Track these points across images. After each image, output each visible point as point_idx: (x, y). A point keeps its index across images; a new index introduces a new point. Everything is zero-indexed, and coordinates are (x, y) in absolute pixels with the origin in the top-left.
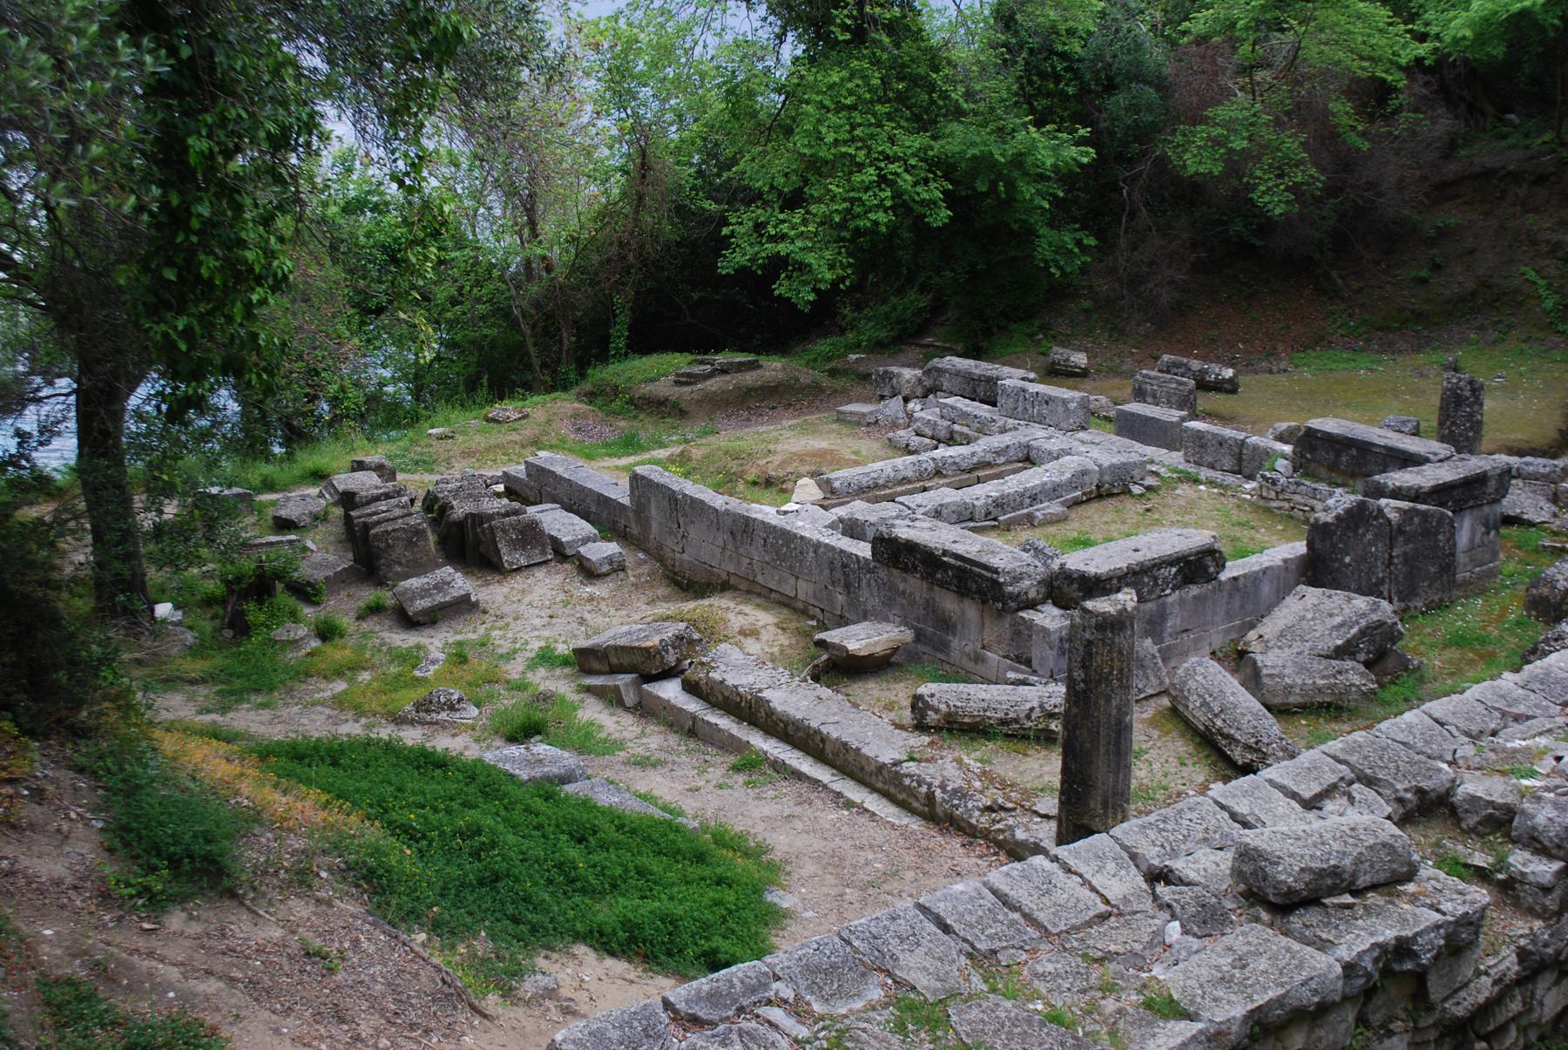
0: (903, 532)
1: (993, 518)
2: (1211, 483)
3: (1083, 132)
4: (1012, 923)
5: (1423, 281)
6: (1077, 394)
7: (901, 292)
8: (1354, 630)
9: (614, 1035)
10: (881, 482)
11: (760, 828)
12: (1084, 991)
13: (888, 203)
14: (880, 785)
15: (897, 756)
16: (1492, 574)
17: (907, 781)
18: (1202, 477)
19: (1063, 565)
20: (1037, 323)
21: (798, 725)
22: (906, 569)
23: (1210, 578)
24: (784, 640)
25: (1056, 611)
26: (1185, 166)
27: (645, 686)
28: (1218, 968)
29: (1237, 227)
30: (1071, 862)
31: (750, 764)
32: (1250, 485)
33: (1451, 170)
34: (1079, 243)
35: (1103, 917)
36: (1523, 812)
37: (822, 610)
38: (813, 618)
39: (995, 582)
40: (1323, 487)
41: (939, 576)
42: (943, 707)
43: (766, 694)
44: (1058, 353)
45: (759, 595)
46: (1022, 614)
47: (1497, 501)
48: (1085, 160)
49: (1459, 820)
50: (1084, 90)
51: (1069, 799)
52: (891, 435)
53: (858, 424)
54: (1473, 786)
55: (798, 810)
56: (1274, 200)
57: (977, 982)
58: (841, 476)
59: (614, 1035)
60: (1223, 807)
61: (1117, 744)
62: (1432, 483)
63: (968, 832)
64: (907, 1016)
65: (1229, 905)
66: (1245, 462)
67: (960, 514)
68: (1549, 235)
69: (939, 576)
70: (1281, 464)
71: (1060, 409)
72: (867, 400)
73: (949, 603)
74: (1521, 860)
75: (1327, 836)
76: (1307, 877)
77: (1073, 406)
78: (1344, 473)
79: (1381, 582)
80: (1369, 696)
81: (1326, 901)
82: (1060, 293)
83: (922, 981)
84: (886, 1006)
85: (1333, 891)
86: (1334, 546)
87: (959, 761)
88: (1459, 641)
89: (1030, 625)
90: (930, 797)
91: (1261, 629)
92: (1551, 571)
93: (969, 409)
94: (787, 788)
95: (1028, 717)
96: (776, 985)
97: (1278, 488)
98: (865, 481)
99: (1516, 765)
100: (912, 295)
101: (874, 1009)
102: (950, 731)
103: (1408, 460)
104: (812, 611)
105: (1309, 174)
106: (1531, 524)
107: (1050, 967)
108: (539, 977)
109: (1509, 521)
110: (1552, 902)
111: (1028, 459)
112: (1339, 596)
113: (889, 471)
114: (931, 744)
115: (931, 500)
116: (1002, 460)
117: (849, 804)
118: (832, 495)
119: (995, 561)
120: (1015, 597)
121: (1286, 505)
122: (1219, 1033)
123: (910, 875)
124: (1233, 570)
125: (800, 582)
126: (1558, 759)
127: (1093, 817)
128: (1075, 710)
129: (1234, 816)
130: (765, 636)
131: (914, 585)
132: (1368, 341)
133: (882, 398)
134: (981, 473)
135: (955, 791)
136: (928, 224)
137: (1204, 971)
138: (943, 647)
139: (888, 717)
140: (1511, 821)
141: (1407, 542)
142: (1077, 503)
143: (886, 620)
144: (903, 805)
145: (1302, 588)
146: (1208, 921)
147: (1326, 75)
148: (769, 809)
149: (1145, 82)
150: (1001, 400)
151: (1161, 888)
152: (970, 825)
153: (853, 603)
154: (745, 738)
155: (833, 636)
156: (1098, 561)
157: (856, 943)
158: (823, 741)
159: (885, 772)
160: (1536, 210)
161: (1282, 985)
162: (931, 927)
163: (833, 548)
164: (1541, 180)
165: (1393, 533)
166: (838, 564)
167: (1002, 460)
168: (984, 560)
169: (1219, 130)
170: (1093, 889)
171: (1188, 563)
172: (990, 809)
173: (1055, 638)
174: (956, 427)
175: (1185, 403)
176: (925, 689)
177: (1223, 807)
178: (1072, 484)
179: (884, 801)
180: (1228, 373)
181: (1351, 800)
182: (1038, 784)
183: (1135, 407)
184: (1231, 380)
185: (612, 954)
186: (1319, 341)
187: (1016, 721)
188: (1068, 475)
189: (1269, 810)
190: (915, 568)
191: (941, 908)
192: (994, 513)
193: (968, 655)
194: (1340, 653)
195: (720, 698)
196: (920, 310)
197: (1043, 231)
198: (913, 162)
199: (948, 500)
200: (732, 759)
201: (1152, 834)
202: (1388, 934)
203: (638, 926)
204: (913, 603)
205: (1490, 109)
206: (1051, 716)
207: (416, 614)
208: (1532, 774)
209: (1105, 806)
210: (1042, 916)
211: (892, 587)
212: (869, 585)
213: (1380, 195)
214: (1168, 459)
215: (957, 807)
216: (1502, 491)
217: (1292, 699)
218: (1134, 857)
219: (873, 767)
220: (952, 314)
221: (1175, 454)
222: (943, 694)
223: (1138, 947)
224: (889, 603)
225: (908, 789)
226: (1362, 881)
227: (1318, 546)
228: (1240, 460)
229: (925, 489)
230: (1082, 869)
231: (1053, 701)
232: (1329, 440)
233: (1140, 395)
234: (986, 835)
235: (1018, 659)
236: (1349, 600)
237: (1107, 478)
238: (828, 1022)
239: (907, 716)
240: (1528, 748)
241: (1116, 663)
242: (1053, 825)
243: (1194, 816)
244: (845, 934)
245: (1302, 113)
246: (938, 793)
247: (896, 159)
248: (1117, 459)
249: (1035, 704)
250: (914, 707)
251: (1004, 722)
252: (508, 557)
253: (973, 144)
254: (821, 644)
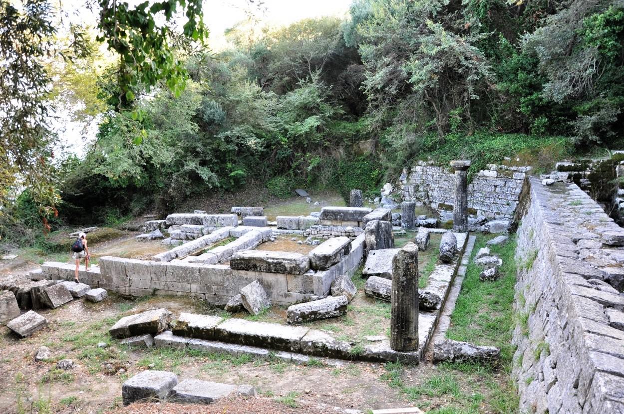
19: (314, 255)
27: (155, 337)
37: (205, 294)
43: (220, 327)
73: (270, 278)
97: (318, 230)
121: (321, 235)
174: (188, 234)
207: (23, 333)
212: (228, 280)
252: (56, 302)
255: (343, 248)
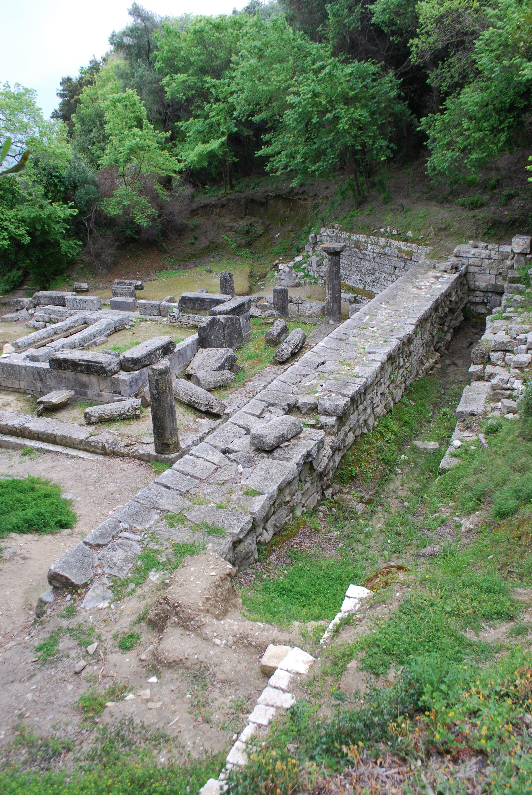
0: (61, 355)
1: (82, 345)
2: (152, 320)
3: (71, 204)
4: (189, 480)
5: (193, 244)
6: (96, 297)
7: (10, 271)
8: (223, 360)
9: (73, 560)
10: (36, 340)
11: (44, 474)
12: (224, 495)
13: (7, 237)
14: (82, 447)
15: (86, 436)
16: (250, 335)
17: (93, 444)
18: (148, 319)
19: (124, 357)
20: (65, 275)
21: (43, 434)
22: (65, 369)
23: (172, 352)
24: (21, 404)
25: (125, 373)
26: (109, 213)
28: (261, 475)
29: (129, 232)
30: (198, 454)
31: (28, 452)
32: (165, 319)
33: (194, 206)
34: (76, 244)
35: (216, 470)
36: (321, 404)
38: (29, 394)
39: (102, 367)
40: (190, 315)
41: (79, 369)
42: (97, 415)
43: (26, 425)
44: (77, 285)
45: (4, 390)
46: (114, 376)
47: (248, 311)
48: (75, 214)
49: (301, 411)
50: (67, 188)
51: (158, 435)
52: (26, 323)
53: (11, 321)
54: (303, 400)
55: (55, 464)
56: (142, 221)
57: (188, 503)
58: (20, 340)
59: (73, 560)
60: (235, 424)
61: (172, 412)
62: (230, 308)
63: (122, 456)
64: (172, 521)
65: (253, 455)
66: (161, 312)
67: (70, 346)
68: (229, 224)
69: (79, 369)
70: (176, 310)
71: (91, 303)
72: (11, 312)
73: (84, 378)
74: (323, 419)
75: (276, 425)
76: (276, 439)
77: (95, 302)
78: (197, 310)
79: (223, 343)
80: (233, 380)
81: (281, 446)
82: (72, 263)
83: (171, 508)
84: (162, 520)
85: (282, 442)
86: (208, 334)
87: (109, 432)
88: (250, 357)
89: (118, 380)
90: (104, 447)
91: (191, 365)
92: (271, 330)
93: (55, 309)
94: (47, 457)
95: (128, 411)
96: (121, 524)
98: (30, 341)
99: (310, 390)
100: (15, 272)
101: (158, 522)
102: (101, 422)
103: (218, 302)
104: (28, 392)
105: (152, 211)
106: (256, 317)
107: (209, 491)
108: (9, 549)
109: (251, 316)
110: (335, 430)
111: (86, 323)
112: (214, 350)
113: (38, 336)
114: (96, 428)
115: (59, 343)
116: (76, 325)
117: (73, 457)
118: (18, 348)
119: (99, 360)
120: (110, 371)
121: (180, 324)
122: (272, 496)
123: (108, 475)
124: (179, 347)
125: (21, 382)
126: (322, 386)
127: (168, 439)
128: (155, 405)
129: (239, 426)
130: (13, 405)
131: (69, 374)
132: (179, 266)
133: (17, 310)
134: (71, 331)
135: (112, 443)
136: (23, 244)
137: (258, 478)
138: (85, 394)
139: (76, 423)
140: (317, 407)
141: (228, 328)
142: (109, 335)
143: (59, 389)
144: (93, 452)
145: (200, 350)
146: (249, 462)
147: (152, 176)
148: (44, 466)
149: (89, 184)
150: (67, 304)
151: (227, 454)
152: (121, 453)
153: (45, 385)
154: (23, 443)
155: (44, 398)
156: (135, 353)
157: (141, 502)
158: (55, 437)
159: (83, 442)
160: (223, 216)
161: (283, 475)
162: (164, 489)
163: (32, 367)
164: (223, 206)
165: (224, 326)
166: (36, 372)
167: (76, 325)
168: (95, 360)
169: (119, 199)
170: (209, 461)
171: (164, 348)
172: (127, 446)
173: (128, 382)
174: (52, 316)
175: (132, 295)
176: (88, 410)
177: (235, 424)
178: (106, 329)
179: (85, 452)
180: (139, 283)
181: (270, 412)
182: (140, 433)
183: (115, 299)
184: (141, 285)
185: (24, 533)
186: (163, 268)
187: (124, 414)
188: (104, 326)
189: (249, 422)
190: (68, 368)
191: (164, 481)
192: (82, 344)
193: (95, 395)
194: (221, 368)
195: (7, 431)
196: (19, 277)
197: (62, 241)
198: (13, 220)
199: (65, 342)
200: (20, 452)
201: (218, 438)
202: (304, 452)
203: (31, 520)
204: (69, 380)
205: (200, 184)
206: (136, 409)
208: (317, 392)
209: (171, 435)
210: (197, 475)
211: (60, 377)
213: (174, 216)
214: (135, 315)
215: (115, 448)
216: (249, 308)
217: (211, 386)
218: (215, 447)
219: (78, 442)
220: (32, 276)
221: (136, 313)
222: (95, 410)
223: (233, 476)
224: (60, 383)
225: (95, 447)
226: (289, 437)
227: (202, 334)
228: (160, 311)
229: (52, 341)
230: (202, 456)
231: (135, 404)
232: (190, 299)
233: (115, 294)
234: (128, 455)
235: (115, 393)
236: (218, 350)
237: (117, 325)
238: (145, 532)
239: (83, 421)
240: (312, 384)
241: (167, 386)
242: (153, 445)
243: (227, 429)
244: (136, 500)
245: (144, 191)
246: (106, 445)
247: (6, 220)
248: (119, 318)
249: (130, 406)
250: (85, 417)
251: (120, 415)
253: (33, 212)
254: (41, 402)
255: (162, 347)
